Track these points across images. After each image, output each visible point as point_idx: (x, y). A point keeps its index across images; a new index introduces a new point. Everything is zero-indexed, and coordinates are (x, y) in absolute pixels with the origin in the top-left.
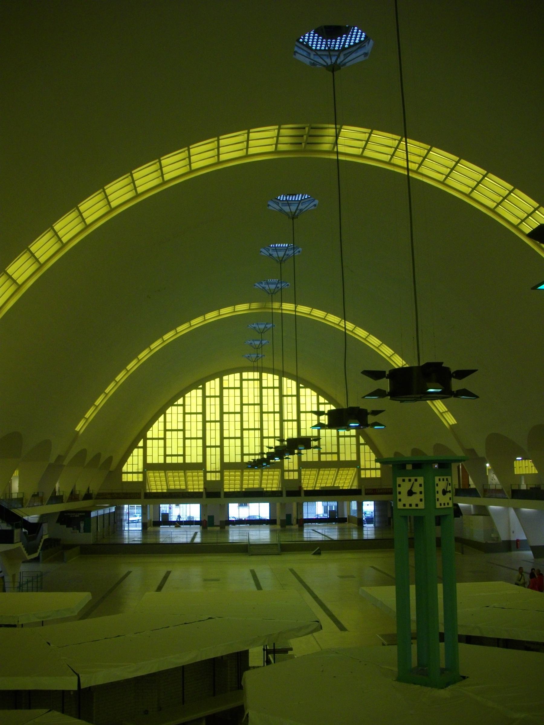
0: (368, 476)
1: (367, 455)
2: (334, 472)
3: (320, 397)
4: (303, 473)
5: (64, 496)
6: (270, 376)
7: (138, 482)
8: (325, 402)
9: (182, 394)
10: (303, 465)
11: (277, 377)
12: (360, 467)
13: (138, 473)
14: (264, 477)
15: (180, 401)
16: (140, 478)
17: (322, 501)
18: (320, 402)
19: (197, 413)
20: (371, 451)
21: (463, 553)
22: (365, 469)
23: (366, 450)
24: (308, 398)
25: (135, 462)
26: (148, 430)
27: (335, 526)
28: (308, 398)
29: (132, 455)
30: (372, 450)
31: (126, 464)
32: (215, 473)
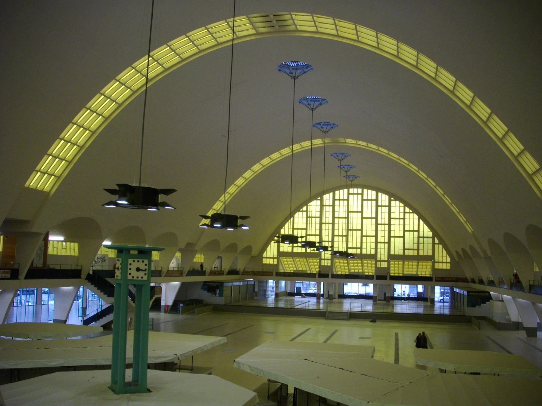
0: (440, 267)
1: (440, 252)
3: (406, 207)
4: (392, 262)
5: (206, 271)
6: (370, 191)
7: (273, 265)
8: (410, 211)
9: (306, 203)
10: (281, 254)
11: (374, 192)
13: (274, 258)
14: (405, 266)
15: (305, 208)
16: (275, 261)
17: (440, 286)
18: (406, 211)
19: (316, 217)
21: (479, 329)
22: (438, 262)
23: (439, 248)
24: (397, 208)
25: (272, 250)
26: (282, 228)
27: (422, 303)
28: (397, 208)
29: (270, 245)
30: (444, 249)
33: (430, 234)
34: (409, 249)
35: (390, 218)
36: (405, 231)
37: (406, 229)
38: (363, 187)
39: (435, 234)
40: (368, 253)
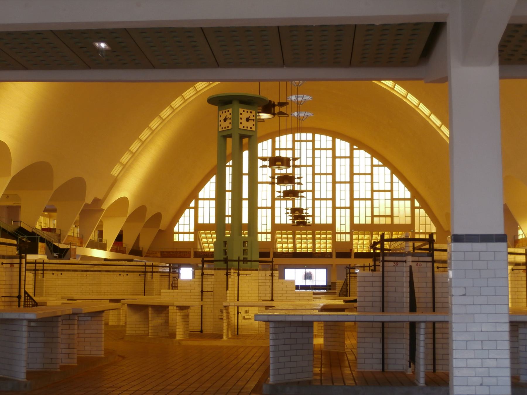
1: (422, 219)
2: (389, 236)
3: (374, 159)
4: (355, 237)
6: (323, 137)
7: (189, 243)
8: (380, 164)
11: (330, 138)
12: (414, 231)
13: (189, 233)
18: (374, 163)
20: (427, 215)
25: (187, 222)
29: (183, 215)
31: (178, 224)
32: (266, 235)
33: (408, 195)
34: (379, 216)
35: (352, 174)
36: (372, 191)
37: (375, 189)
38: (314, 131)
39: (415, 195)
40: (323, 222)
